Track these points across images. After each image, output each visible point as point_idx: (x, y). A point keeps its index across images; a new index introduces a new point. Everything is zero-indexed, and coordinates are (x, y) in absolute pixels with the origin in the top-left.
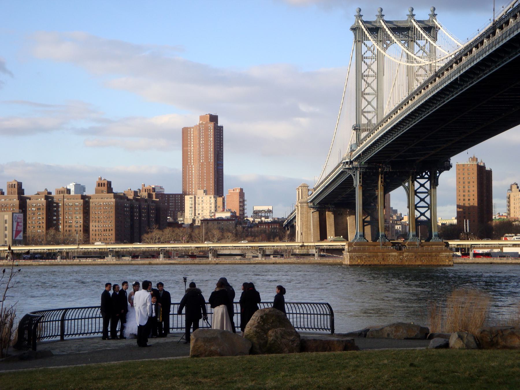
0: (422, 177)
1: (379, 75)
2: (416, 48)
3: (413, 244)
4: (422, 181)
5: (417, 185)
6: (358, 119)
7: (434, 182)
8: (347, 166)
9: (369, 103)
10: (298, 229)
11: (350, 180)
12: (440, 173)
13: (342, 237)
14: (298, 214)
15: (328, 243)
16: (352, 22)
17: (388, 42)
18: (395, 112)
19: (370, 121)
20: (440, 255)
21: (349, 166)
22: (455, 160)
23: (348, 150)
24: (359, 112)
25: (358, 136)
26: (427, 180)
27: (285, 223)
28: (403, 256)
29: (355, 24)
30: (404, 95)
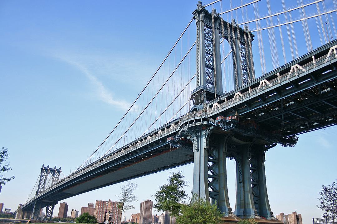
1: (45, 180)
2: (55, 175)
4: (51, 206)
5: (49, 207)
6: (38, 190)
11: (33, 205)
15: (24, 220)
16: (41, 167)
18: (48, 189)
22: (59, 202)
24: (39, 188)
27: (13, 214)
30: (50, 186)
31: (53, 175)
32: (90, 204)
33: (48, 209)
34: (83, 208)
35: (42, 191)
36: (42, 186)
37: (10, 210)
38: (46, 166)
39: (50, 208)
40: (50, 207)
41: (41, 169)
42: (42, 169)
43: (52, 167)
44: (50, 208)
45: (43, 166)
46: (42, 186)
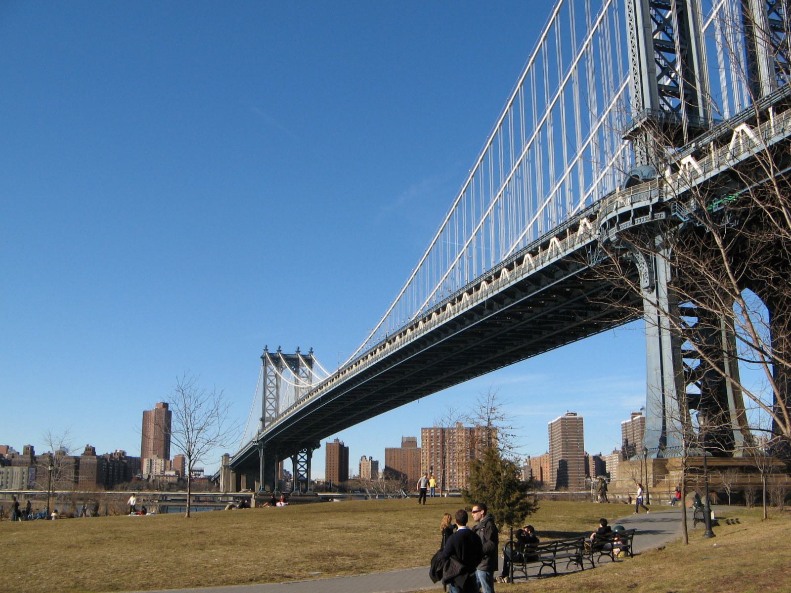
0: (302, 452)
1: (277, 387)
2: (301, 371)
4: (302, 455)
5: (299, 457)
6: (264, 414)
7: (310, 456)
10: (221, 483)
11: (257, 453)
12: (313, 450)
15: (243, 492)
18: (289, 410)
19: (271, 415)
22: (323, 442)
23: (256, 433)
24: (264, 410)
25: (263, 425)
27: (213, 479)
30: (292, 402)
31: (296, 372)
33: (298, 462)
34: (388, 451)
35: (274, 416)
36: (271, 404)
38: (273, 350)
39: (302, 460)
40: (302, 456)
42: (264, 358)
43: (290, 350)
44: (302, 460)
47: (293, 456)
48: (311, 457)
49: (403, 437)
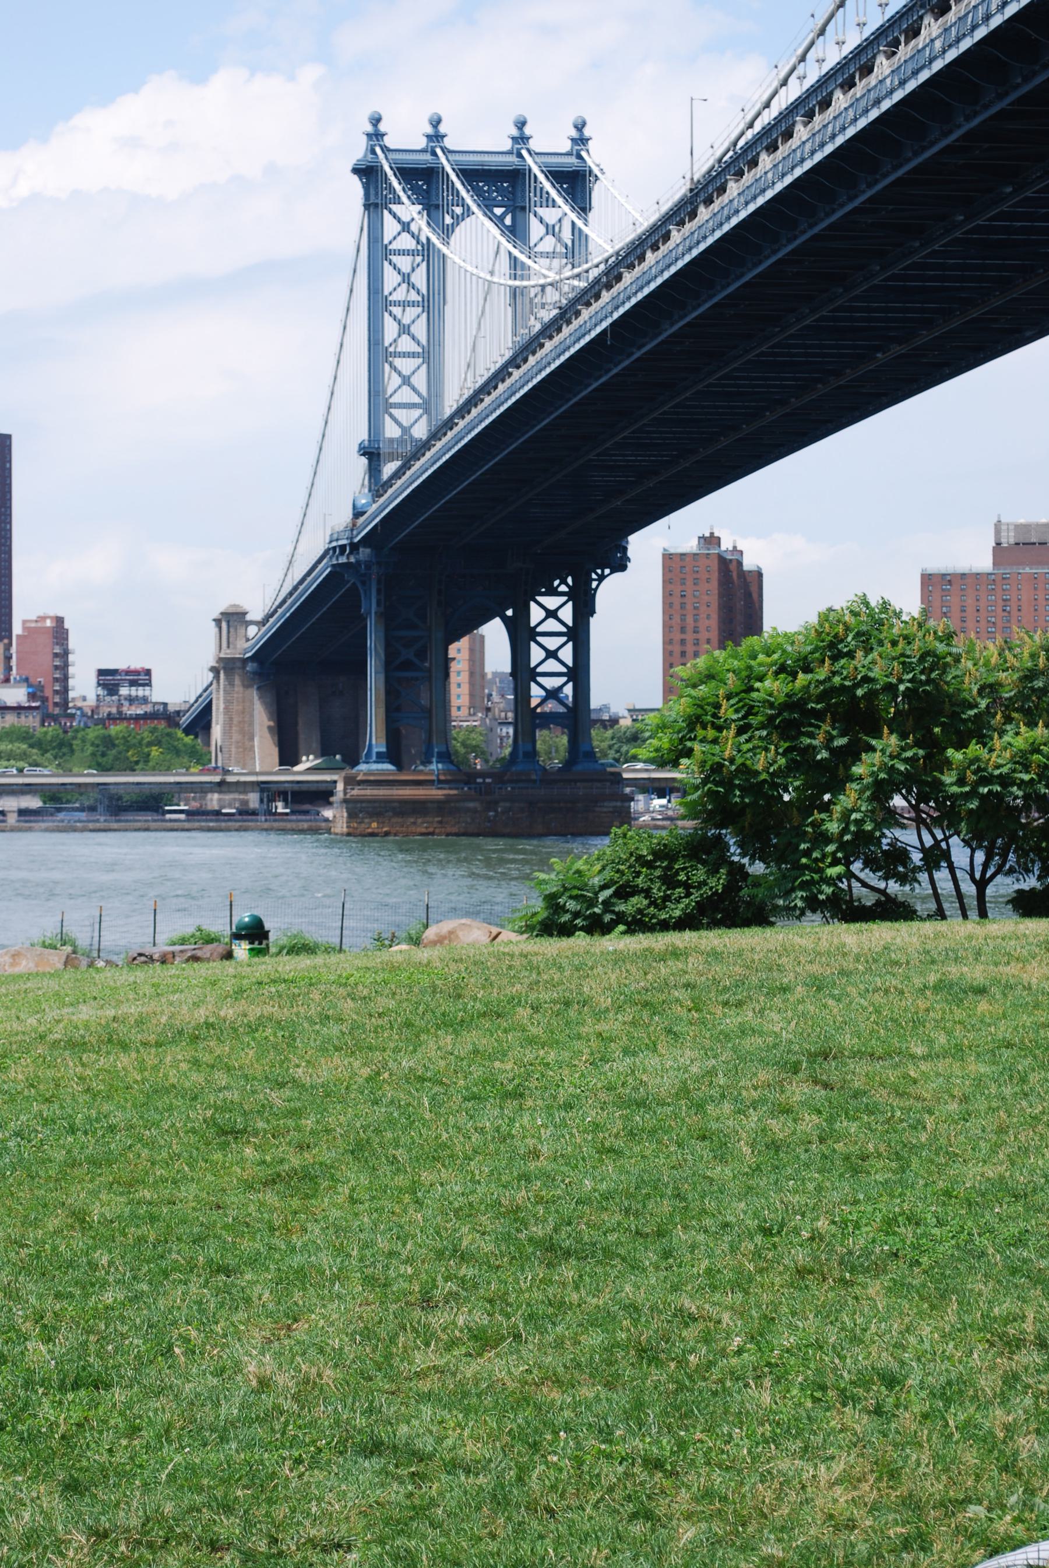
0: (553, 592)
2: (536, 230)
3: (524, 778)
4: (551, 602)
5: (536, 614)
7: (584, 606)
8: (343, 560)
9: (406, 381)
13: (338, 757)
14: (218, 690)
16: (358, 151)
17: (458, 210)
19: (406, 430)
20: (597, 809)
21: (348, 558)
25: (374, 470)
26: (565, 598)
28: (496, 811)
29: (365, 156)
31: (516, 232)
32: (1025, 528)
33: (533, 634)
37: (142, 677)
41: (356, 187)
42: (368, 173)
44: (552, 625)
45: (376, 136)
46: (406, 381)
47: (509, 613)
48: (592, 612)
49: (998, 526)
